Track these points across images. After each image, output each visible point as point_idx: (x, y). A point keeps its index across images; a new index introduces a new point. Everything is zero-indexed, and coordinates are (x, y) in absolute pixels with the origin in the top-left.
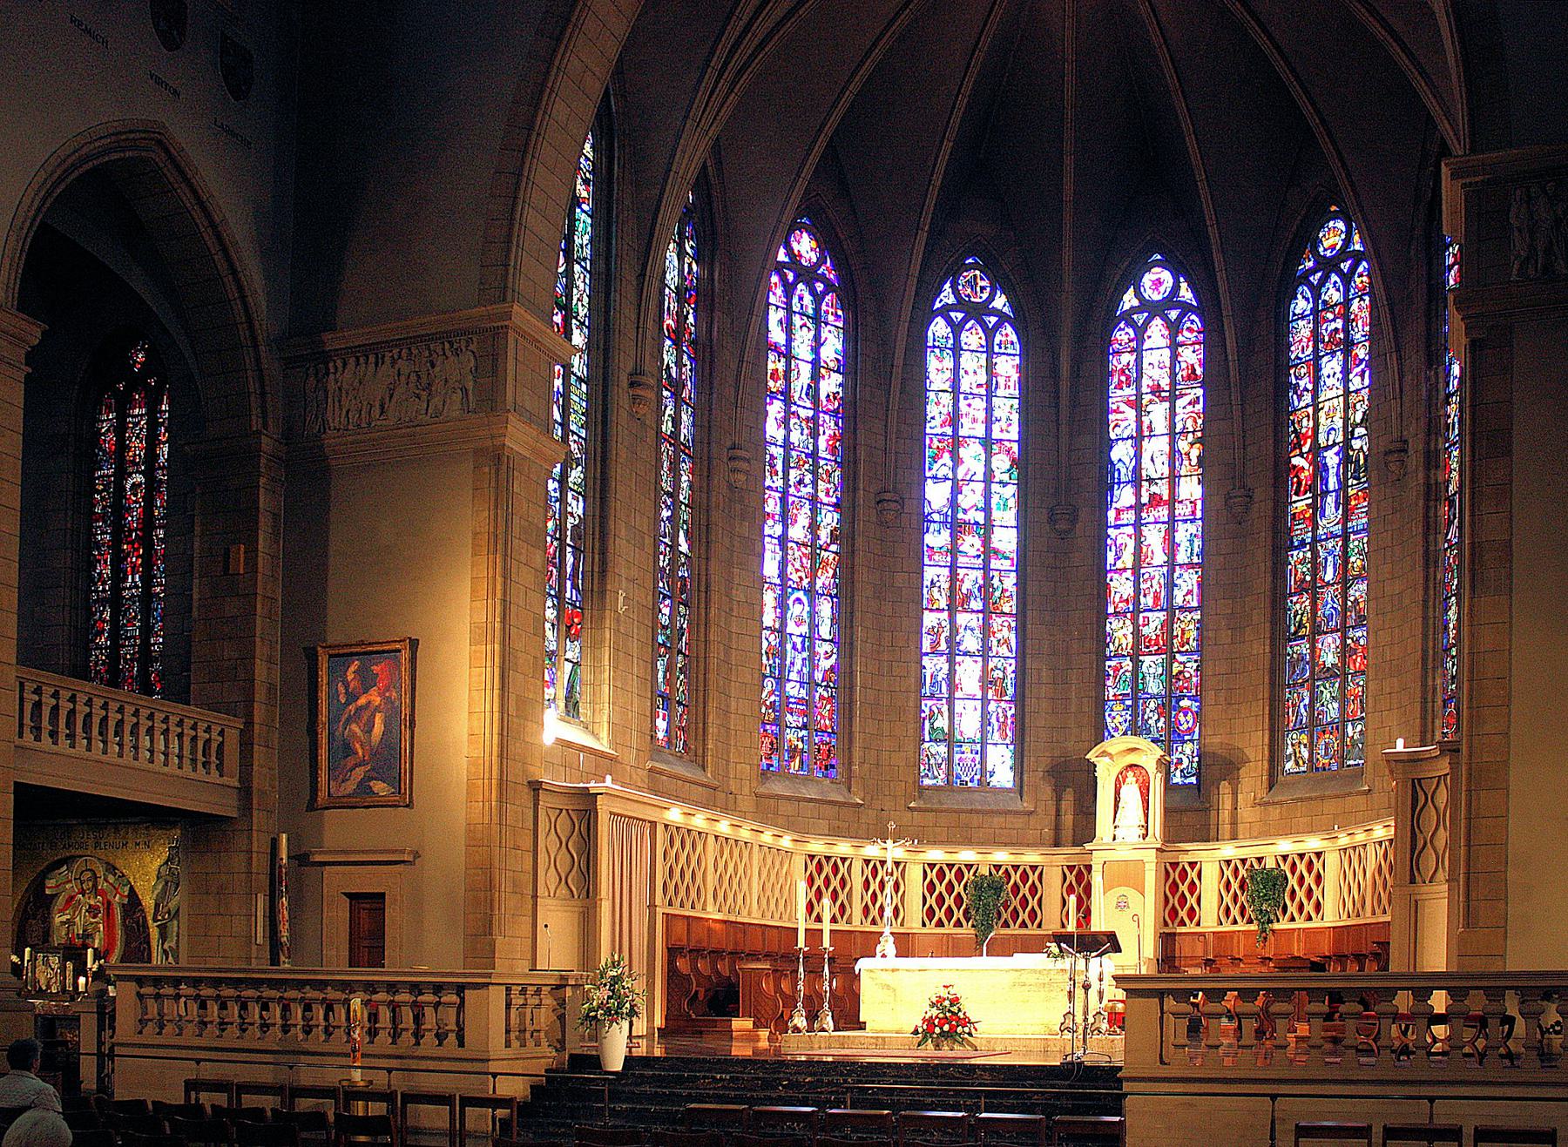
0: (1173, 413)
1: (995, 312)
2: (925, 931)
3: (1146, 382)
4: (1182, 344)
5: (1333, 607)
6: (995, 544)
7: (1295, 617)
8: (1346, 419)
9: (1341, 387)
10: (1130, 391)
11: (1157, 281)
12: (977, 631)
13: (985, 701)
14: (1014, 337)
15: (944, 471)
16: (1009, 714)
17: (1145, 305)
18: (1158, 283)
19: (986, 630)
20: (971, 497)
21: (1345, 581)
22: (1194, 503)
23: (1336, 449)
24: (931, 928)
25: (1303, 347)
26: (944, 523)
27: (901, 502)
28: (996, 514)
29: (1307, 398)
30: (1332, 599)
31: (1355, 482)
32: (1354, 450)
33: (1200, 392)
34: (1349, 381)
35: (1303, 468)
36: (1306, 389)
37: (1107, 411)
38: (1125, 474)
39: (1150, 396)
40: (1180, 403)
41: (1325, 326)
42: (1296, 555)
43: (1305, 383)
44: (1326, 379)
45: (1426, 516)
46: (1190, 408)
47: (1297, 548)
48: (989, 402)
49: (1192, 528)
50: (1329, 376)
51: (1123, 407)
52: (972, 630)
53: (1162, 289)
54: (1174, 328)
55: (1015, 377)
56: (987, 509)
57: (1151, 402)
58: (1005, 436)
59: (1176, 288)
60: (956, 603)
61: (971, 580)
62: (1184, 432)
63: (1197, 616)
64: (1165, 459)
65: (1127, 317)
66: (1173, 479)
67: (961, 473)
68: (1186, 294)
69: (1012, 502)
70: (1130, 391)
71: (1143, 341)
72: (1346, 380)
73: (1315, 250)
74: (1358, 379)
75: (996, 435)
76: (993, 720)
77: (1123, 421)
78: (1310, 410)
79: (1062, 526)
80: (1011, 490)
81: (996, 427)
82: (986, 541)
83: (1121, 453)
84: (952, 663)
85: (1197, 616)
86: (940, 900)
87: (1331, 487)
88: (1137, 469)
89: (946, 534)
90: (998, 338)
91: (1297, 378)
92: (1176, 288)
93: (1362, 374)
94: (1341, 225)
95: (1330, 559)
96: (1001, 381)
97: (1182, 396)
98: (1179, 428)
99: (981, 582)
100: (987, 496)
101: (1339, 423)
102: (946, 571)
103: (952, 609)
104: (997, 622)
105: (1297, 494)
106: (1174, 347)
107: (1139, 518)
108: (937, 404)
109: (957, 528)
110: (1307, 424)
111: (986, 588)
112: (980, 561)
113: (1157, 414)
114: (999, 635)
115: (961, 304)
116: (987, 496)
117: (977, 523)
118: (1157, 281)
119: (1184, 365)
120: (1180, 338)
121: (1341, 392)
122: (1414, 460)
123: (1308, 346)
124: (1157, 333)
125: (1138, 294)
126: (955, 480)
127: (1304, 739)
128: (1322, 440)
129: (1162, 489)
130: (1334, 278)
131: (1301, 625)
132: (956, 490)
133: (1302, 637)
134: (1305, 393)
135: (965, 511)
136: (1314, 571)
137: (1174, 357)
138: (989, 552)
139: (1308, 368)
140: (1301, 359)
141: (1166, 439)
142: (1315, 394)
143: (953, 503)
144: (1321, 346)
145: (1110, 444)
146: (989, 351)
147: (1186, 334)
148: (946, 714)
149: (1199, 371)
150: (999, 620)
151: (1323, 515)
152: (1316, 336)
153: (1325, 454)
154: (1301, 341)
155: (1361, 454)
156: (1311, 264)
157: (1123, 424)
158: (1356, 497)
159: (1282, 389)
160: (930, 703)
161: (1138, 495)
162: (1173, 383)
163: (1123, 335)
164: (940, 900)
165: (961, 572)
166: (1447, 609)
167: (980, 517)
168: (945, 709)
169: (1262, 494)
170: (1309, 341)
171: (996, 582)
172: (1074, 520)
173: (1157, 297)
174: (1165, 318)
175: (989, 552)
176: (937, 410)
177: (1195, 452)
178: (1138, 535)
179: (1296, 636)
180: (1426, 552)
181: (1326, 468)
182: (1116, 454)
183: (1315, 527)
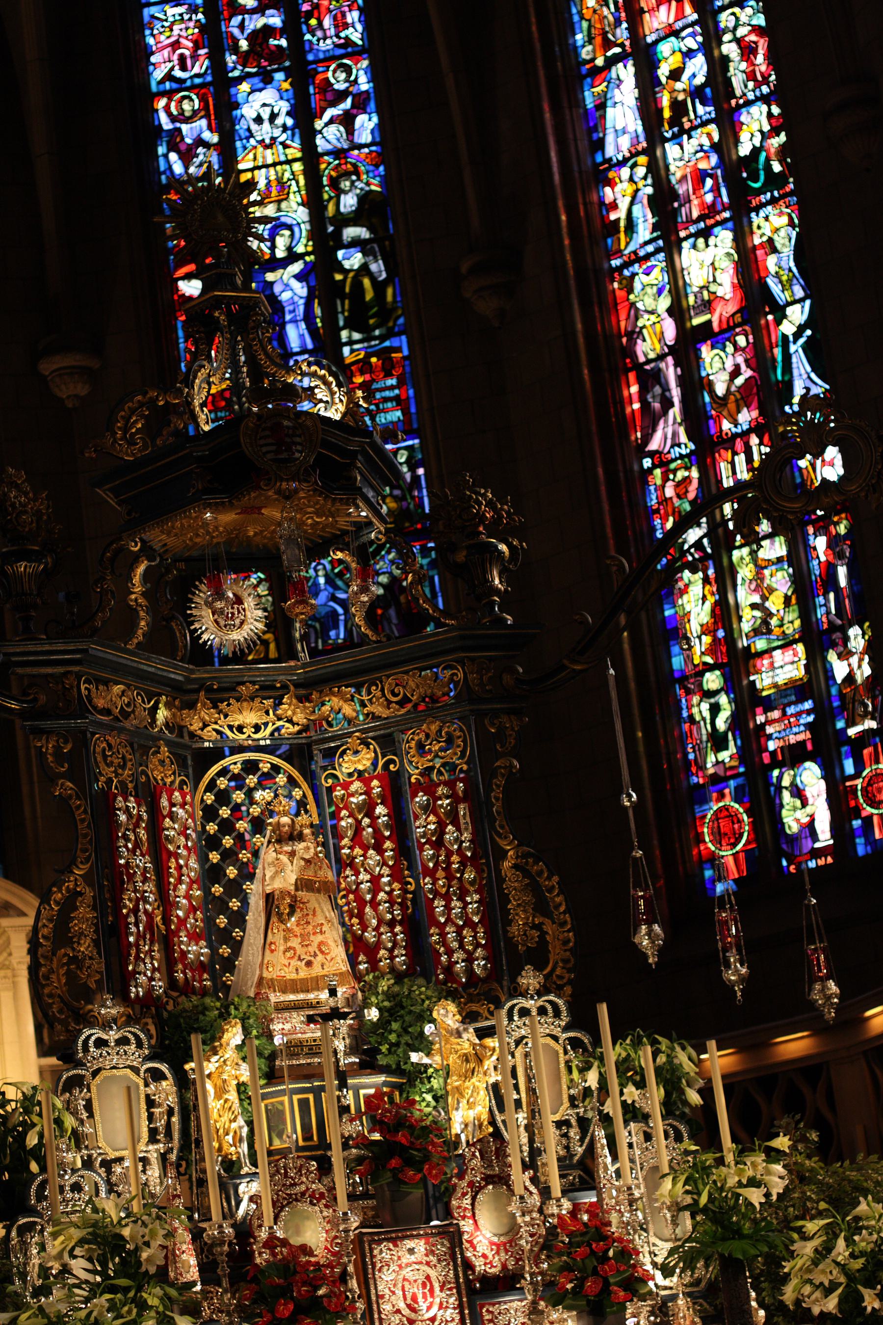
5: (333, 598)
9: (296, 144)
23: (296, 267)
25: (182, 58)
30: (329, 581)
31: (356, 336)
32: (346, 272)
34: (314, 133)
36: (200, 142)
41: (236, 20)
44: (254, 127)
50: (259, 120)
87: (294, 343)
91: (173, 119)
121: (294, 152)
123: (195, 57)
134: (200, 150)
139: (203, 99)
140: (184, 81)
144: (231, 59)
153: (270, 277)
154: (176, 45)
155: (366, 282)
170: (197, 46)
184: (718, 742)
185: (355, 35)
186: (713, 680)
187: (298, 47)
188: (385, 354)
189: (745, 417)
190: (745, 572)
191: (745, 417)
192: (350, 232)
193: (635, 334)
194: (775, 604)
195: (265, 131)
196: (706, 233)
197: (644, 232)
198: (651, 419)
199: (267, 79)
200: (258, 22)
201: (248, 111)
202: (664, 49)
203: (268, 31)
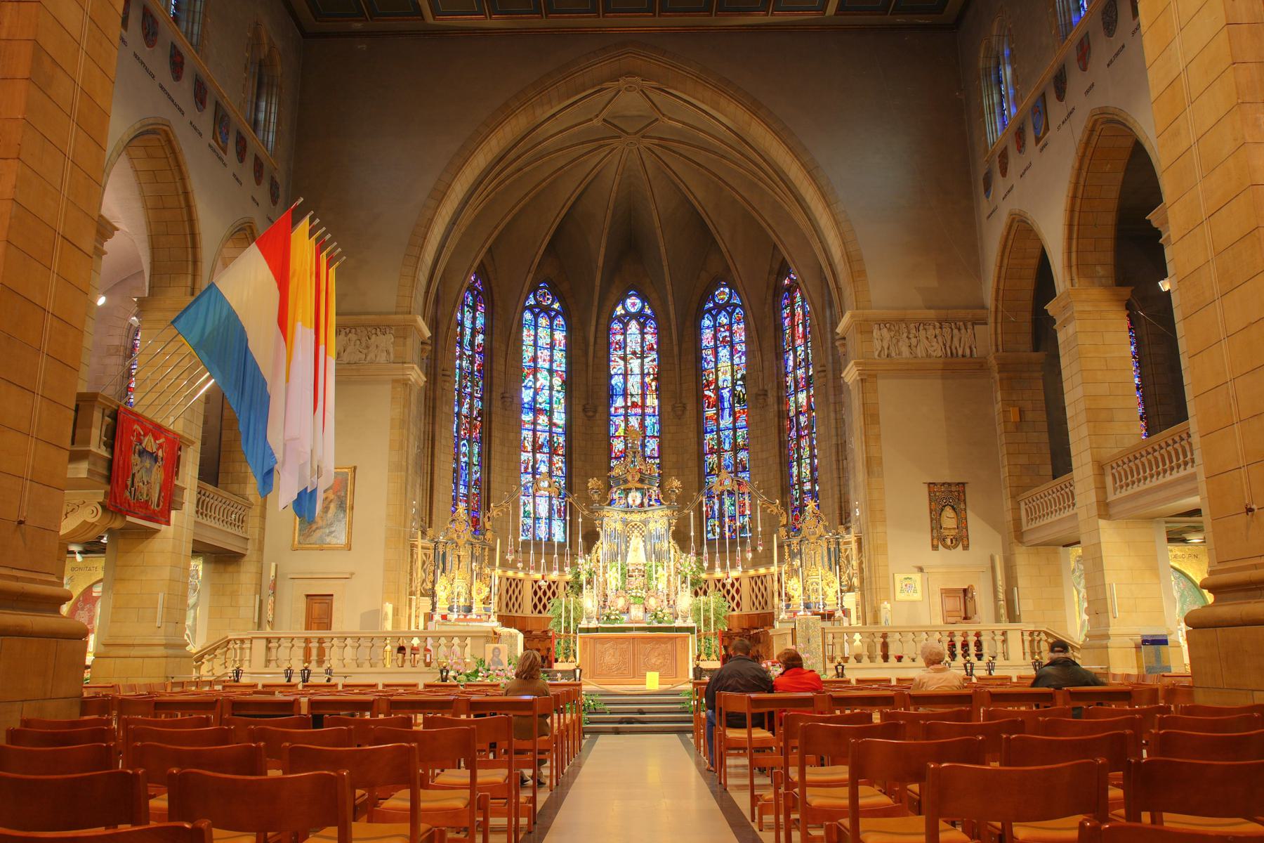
0: (642, 365)
1: (554, 310)
2: (533, 615)
3: (628, 349)
4: (646, 333)
6: (555, 421)
7: (710, 463)
8: (733, 376)
10: (620, 353)
11: (634, 303)
12: (547, 463)
13: (550, 498)
14: (563, 323)
15: (530, 384)
16: (562, 505)
17: (628, 313)
18: (634, 304)
19: (551, 462)
20: (543, 398)
21: (735, 448)
22: (654, 408)
23: (728, 389)
24: (536, 614)
26: (531, 409)
27: (512, 397)
28: (555, 406)
29: (712, 365)
33: (655, 356)
35: (710, 397)
37: (609, 360)
38: (619, 390)
39: (631, 356)
40: (646, 360)
42: (708, 436)
43: (711, 358)
45: (779, 425)
46: (651, 363)
47: (710, 432)
48: (552, 352)
49: (654, 420)
51: (618, 359)
52: (544, 462)
53: (636, 307)
54: (642, 327)
55: (563, 342)
56: (551, 403)
57: (631, 358)
58: (558, 369)
59: (643, 308)
60: (536, 448)
61: (543, 437)
62: (649, 374)
63: (657, 461)
64: (639, 385)
65: (620, 319)
66: (643, 396)
67: (538, 385)
68: (648, 311)
69: (562, 401)
70: (620, 353)
71: (627, 330)
72: (732, 359)
73: (713, 299)
74: (738, 359)
75: (555, 367)
76: (555, 508)
77: (617, 366)
78: (713, 370)
79: (590, 414)
80: (561, 395)
81: (555, 365)
82: (550, 418)
83: (617, 381)
84: (534, 477)
85: (657, 461)
86: (540, 600)
87: (726, 406)
88: (625, 389)
89: (531, 415)
90: (556, 322)
92: (643, 308)
93: (740, 357)
94: (727, 290)
95: (727, 439)
96: (558, 342)
97: (647, 357)
98: (646, 371)
99: (548, 438)
100: (551, 396)
101: (729, 377)
102: (531, 433)
103: (534, 451)
104: (556, 459)
105: (708, 407)
106: (643, 334)
107: (626, 412)
108: (527, 351)
109: (537, 411)
110: (712, 377)
111: (551, 442)
112: (547, 428)
113: (635, 364)
114: (557, 466)
115: (538, 304)
116: (551, 396)
117: (545, 410)
118: (634, 303)
119: (648, 343)
120: (645, 331)
121: (729, 364)
122: (771, 399)
124: (634, 327)
125: (624, 308)
126: (535, 388)
127: (717, 523)
128: (720, 383)
129: (638, 399)
130: (724, 313)
131: (712, 469)
132: (536, 393)
133: (714, 475)
135: (540, 404)
136: (720, 443)
137: (643, 339)
138: (552, 424)
141: (639, 376)
142: (716, 363)
143: (534, 399)
145: (611, 377)
146: (551, 327)
147: (649, 329)
148: (532, 504)
149: (655, 347)
150: (557, 458)
151: (722, 418)
152: (715, 337)
156: (711, 305)
157: (618, 367)
158: (740, 412)
159: (699, 359)
160: (524, 498)
161: (626, 401)
162: (643, 352)
163: (616, 326)
164: (540, 600)
165: (539, 433)
166: (791, 467)
167: (547, 407)
168: (531, 501)
169: (691, 407)
171: (555, 440)
172: (595, 411)
173: (633, 310)
174: (638, 321)
175: (552, 424)
176: (528, 353)
177: (654, 384)
178: (626, 421)
179: (709, 474)
180: (780, 442)
181: (722, 397)
182: (613, 382)
183: (718, 424)
184: (797, 500)
185: (743, 339)
186: (797, 487)
187: (732, 340)
188: (743, 409)
189: (806, 432)
190: (804, 465)
191: (806, 432)
192: (739, 382)
193: (789, 411)
194: (808, 472)
195: (723, 359)
196: (802, 391)
197: (792, 389)
198: (791, 429)
199: (725, 347)
200: (724, 334)
201: (721, 354)
202: (799, 349)
203: (726, 336)
